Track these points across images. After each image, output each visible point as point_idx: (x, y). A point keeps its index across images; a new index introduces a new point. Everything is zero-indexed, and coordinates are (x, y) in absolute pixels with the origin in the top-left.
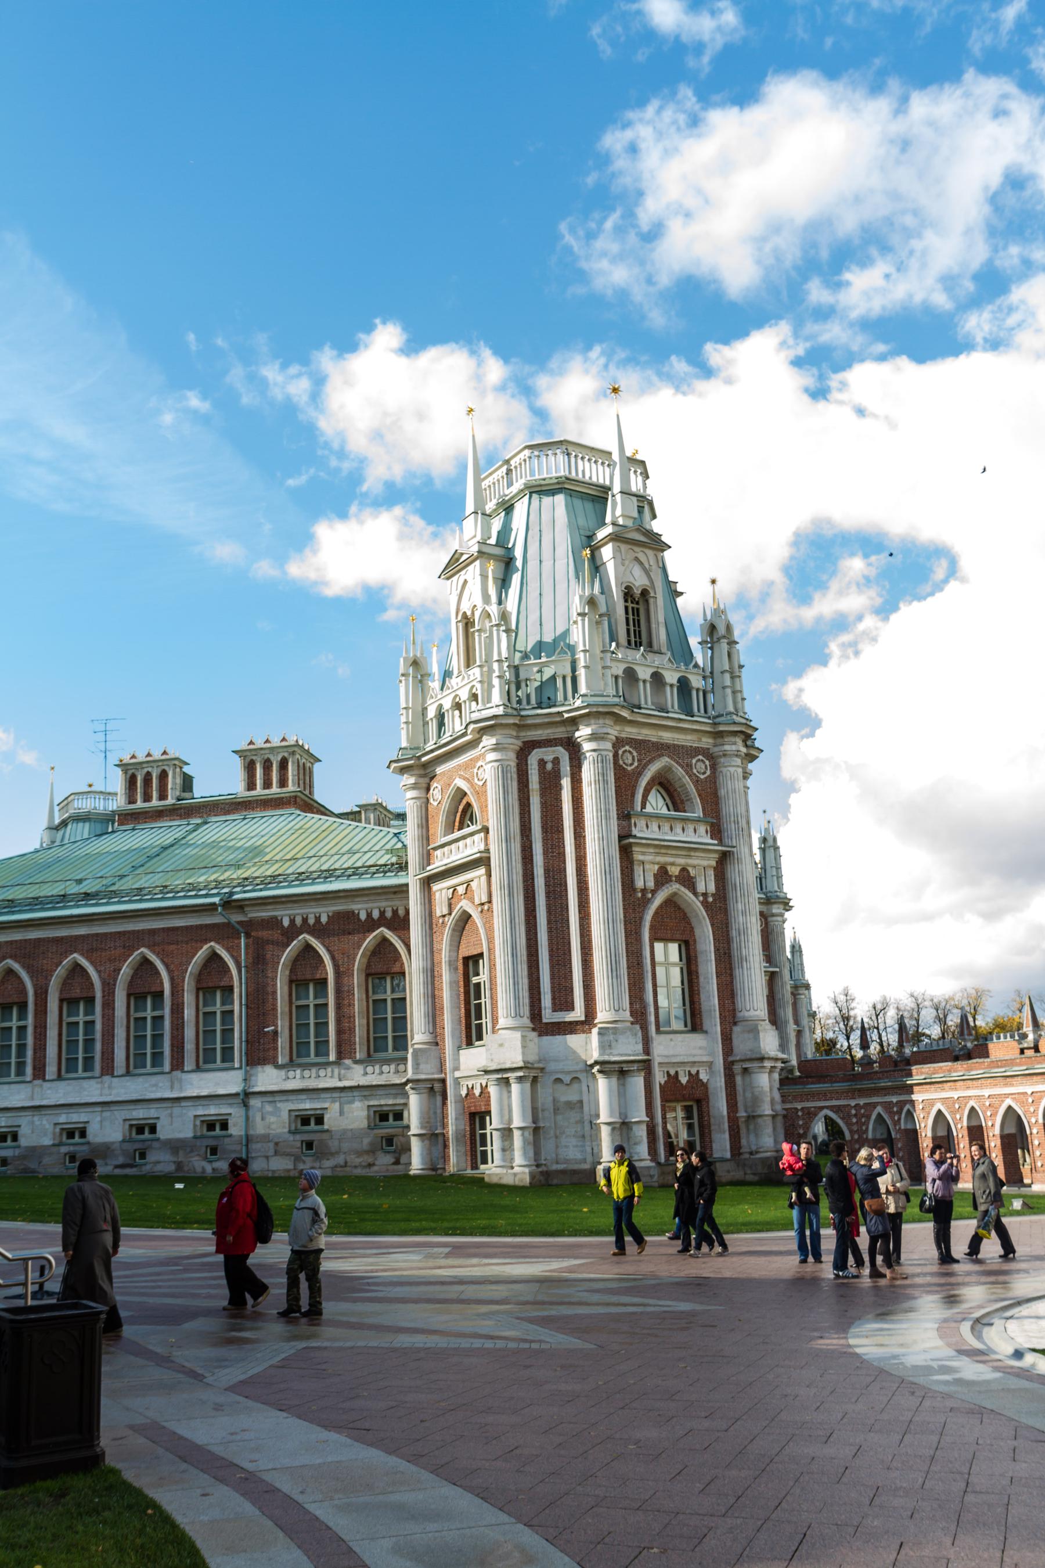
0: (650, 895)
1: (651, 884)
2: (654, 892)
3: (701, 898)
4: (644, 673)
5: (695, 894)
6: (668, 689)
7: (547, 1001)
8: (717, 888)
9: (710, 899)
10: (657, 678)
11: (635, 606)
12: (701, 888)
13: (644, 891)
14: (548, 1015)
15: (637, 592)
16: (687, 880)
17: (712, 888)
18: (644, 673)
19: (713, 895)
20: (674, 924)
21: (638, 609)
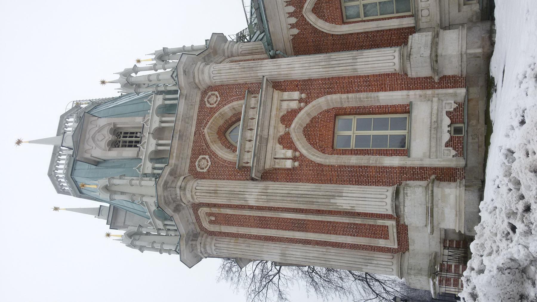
0: (297, 154)
1: (289, 153)
2: (296, 150)
3: (302, 104)
5: (300, 109)
7: (382, 243)
9: (303, 96)
11: (122, 135)
12: (294, 105)
13: (294, 159)
16: (288, 118)
17: (296, 95)
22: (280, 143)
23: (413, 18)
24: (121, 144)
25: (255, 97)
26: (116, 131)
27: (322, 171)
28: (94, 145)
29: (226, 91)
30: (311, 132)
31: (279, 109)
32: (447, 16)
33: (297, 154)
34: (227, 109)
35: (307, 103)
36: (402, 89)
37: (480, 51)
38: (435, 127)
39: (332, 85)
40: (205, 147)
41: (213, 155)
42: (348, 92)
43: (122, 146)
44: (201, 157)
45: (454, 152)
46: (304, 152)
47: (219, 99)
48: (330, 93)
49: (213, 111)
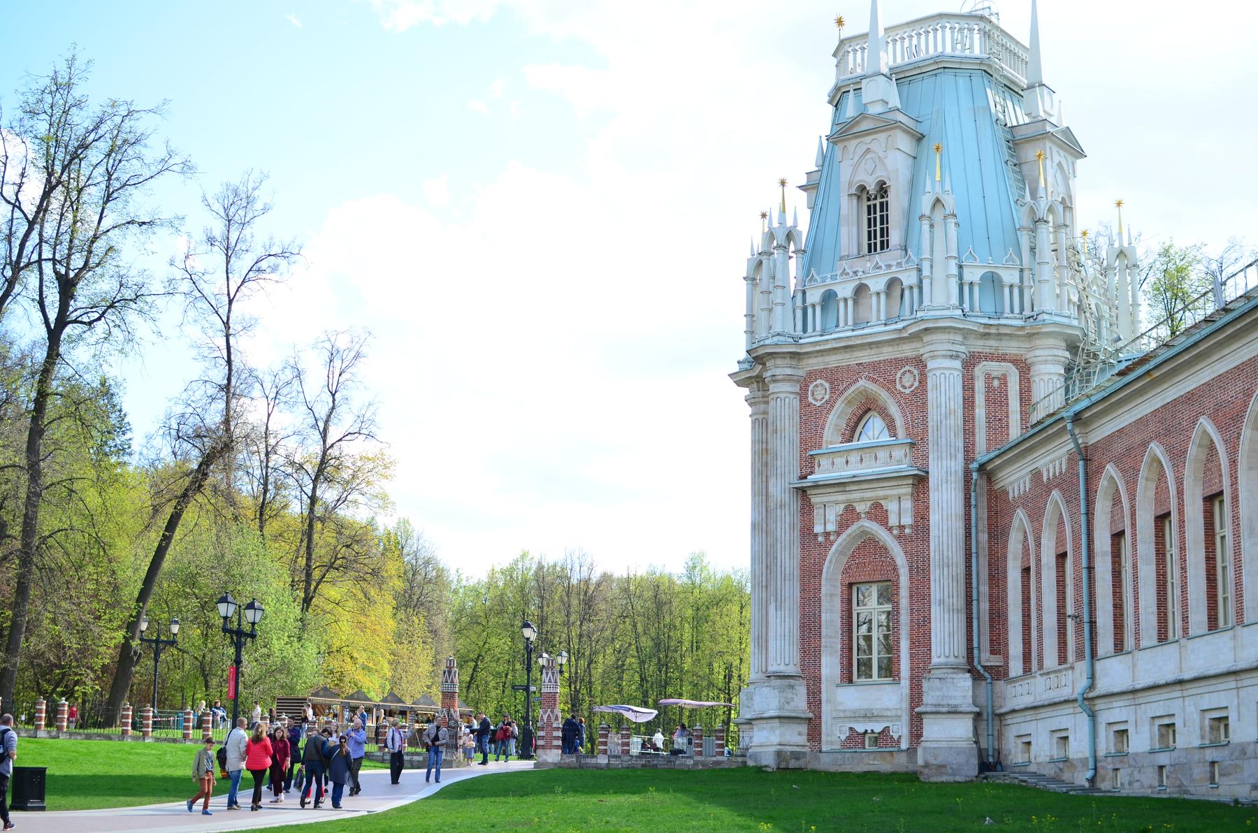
1: (831, 527)
2: (838, 534)
4: (845, 290)
5: (890, 529)
10: (861, 290)
12: (893, 521)
13: (827, 534)
15: (872, 188)
16: (878, 513)
17: (907, 520)
22: (846, 508)
23: (1021, 673)
24: (871, 203)
28: (856, 159)
29: (917, 401)
30: (870, 545)
31: (885, 498)
33: (832, 538)
34: (894, 410)
35: (899, 538)
36: (912, 669)
38: (868, 716)
39: (920, 571)
40: (841, 388)
41: (830, 404)
42: (911, 596)
43: (869, 207)
44: (827, 385)
45: (843, 737)
46: (833, 548)
47: (907, 391)
48: (911, 570)
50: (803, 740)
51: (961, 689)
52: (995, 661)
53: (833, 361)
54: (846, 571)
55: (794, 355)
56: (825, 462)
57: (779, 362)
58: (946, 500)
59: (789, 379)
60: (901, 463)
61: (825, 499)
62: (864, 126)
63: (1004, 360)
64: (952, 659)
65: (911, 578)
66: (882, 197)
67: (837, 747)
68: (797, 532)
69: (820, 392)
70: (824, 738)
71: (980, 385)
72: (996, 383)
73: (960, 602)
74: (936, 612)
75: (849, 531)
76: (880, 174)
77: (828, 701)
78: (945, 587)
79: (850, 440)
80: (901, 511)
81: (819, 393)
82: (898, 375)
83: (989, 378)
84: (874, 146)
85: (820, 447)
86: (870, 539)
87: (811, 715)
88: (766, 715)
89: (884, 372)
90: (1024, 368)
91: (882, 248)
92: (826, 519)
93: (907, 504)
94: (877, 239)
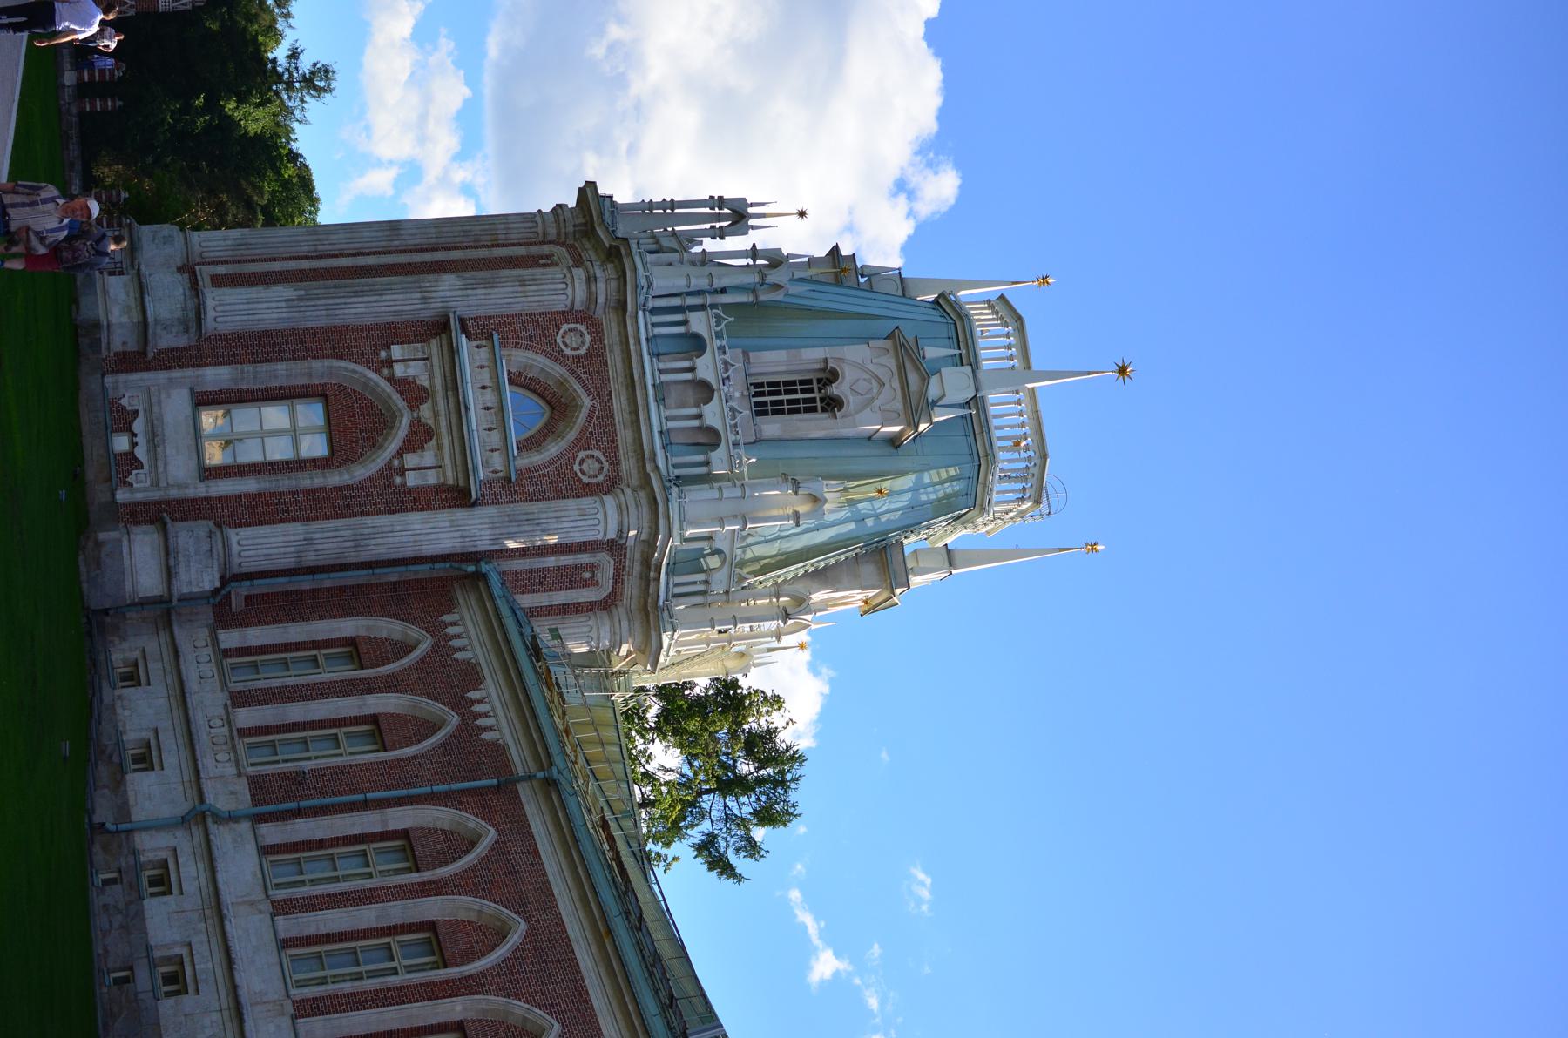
1: (399, 370)
2: (391, 379)
4: (706, 368)
5: (399, 455)
6: (694, 411)
7: (221, 270)
8: (418, 490)
10: (704, 391)
12: (411, 460)
13: (390, 363)
14: (205, 272)
15: (834, 390)
16: (420, 437)
17: (412, 480)
18: (706, 368)
19: (404, 485)
20: (353, 424)
21: (814, 410)
22: (424, 389)
23: (223, 646)
24: (815, 385)
25: (494, 472)
26: (833, 405)
27: (334, 348)
28: (870, 367)
31: (440, 447)
32: (162, 641)
33: (385, 371)
34: (553, 449)
35: (389, 467)
36: (220, 499)
37: (102, 536)
38: (154, 440)
40: (580, 371)
41: (558, 356)
42: (314, 490)
43: (810, 382)
44: (583, 351)
45: (124, 402)
46: (372, 375)
47: (576, 468)
48: (348, 488)
49: (584, 442)
50: (117, 346)
51: (199, 577)
52: (237, 604)
53: (614, 358)
54: (342, 389)
55: (622, 305)
56: (483, 355)
57: (614, 284)
58: (437, 532)
59: (591, 298)
60: (486, 464)
61: (436, 360)
62: (913, 378)
63: (615, 582)
64: (236, 560)
65: (338, 489)
66: (822, 400)
67: (111, 394)
68: (391, 319)
69: (574, 340)
70: (122, 377)
71: (584, 558)
72: (587, 575)
73: (311, 559)
74: (296, 530)
75: (396, 397)
76: (851, 402)
77: (170, 379)
78: (329, 538)
79: (511, 382)
80: (423, 469)
81: (573, 340)
82: (597, 453)
83: (593, 567)
84: (887, 393)
85: (503, 345)
86: (385, 422)
87: (151, 355)
88: (147, 299)
89: (600, 433)
90: (606, 605)
91: (756, 404)
92: (410, 362)
93: (432, 478)
94: (773, 398)
